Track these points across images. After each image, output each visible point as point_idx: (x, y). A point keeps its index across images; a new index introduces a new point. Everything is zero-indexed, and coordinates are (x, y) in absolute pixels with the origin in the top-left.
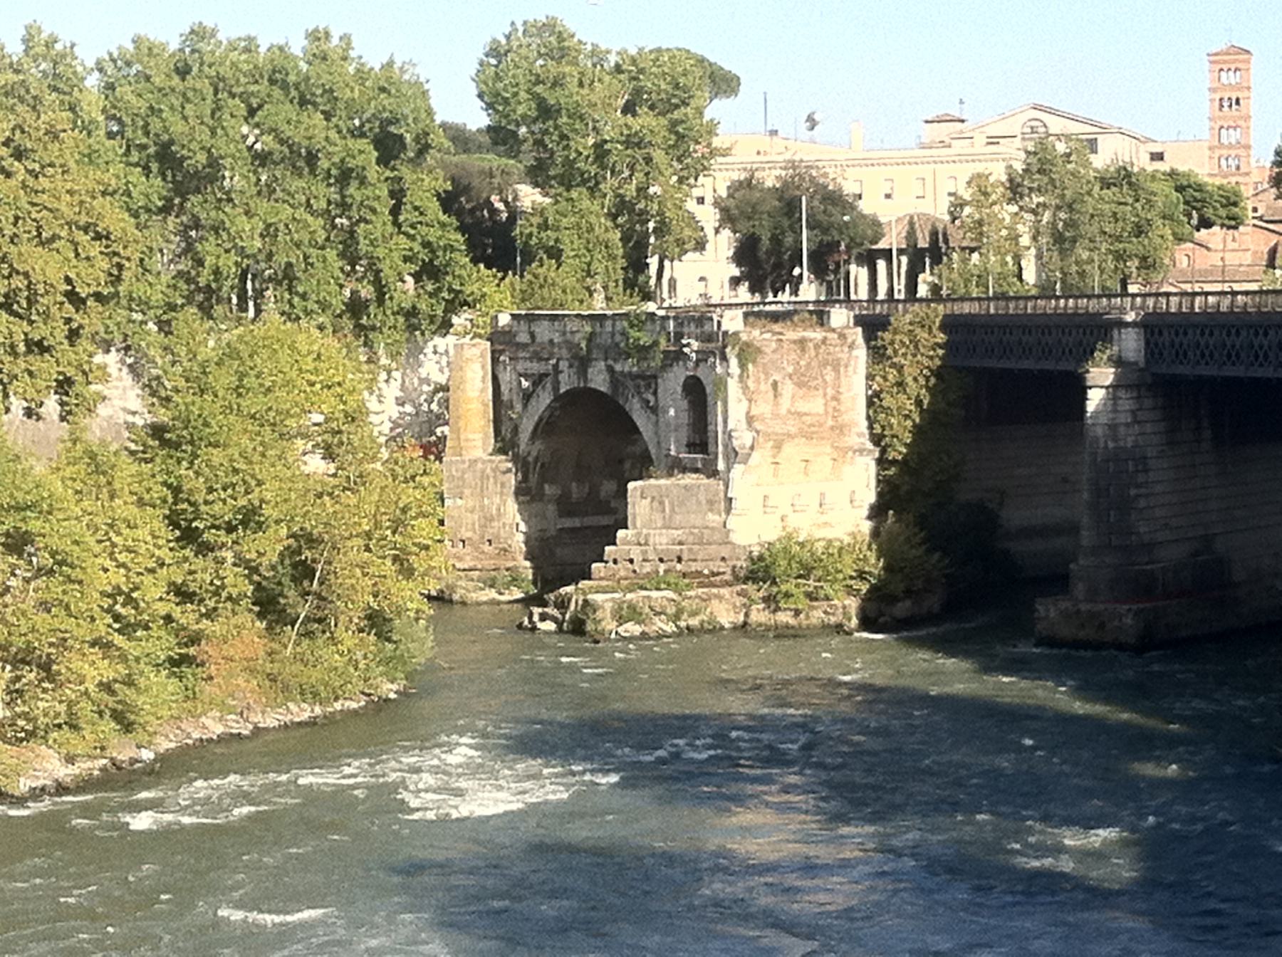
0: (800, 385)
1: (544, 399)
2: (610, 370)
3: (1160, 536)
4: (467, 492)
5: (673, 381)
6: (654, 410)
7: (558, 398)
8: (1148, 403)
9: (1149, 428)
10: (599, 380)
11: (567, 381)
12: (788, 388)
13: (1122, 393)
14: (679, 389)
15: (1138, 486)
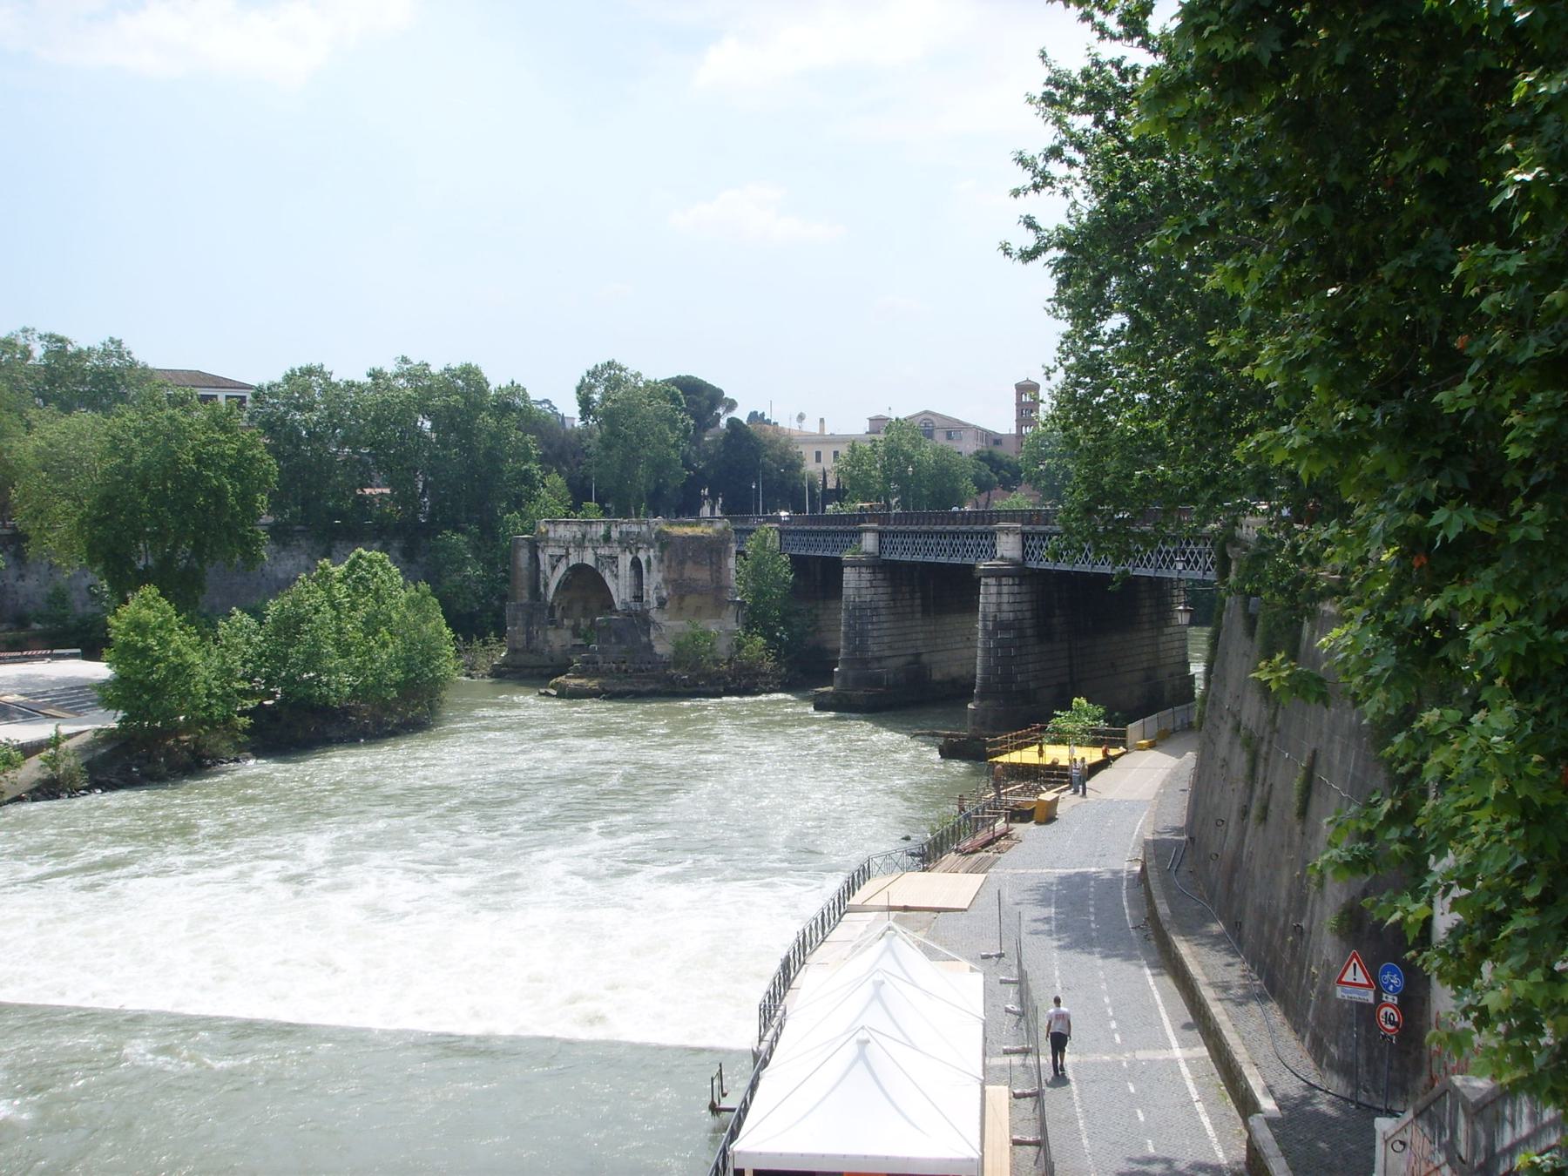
0: (696, 563)
1: (562, 569)
2: (596, 554)
3: (887, 653)
4: (519, 622)
5: (625, 560)
6: (616, 576)
7: (569, 569)
8: (880, 576)
9: (881, 590)
10: (589, 559)
11: (573, 560)
12: (689, 565)
13: (863, 570)
14: (629, 564)
15: (872, 623)
